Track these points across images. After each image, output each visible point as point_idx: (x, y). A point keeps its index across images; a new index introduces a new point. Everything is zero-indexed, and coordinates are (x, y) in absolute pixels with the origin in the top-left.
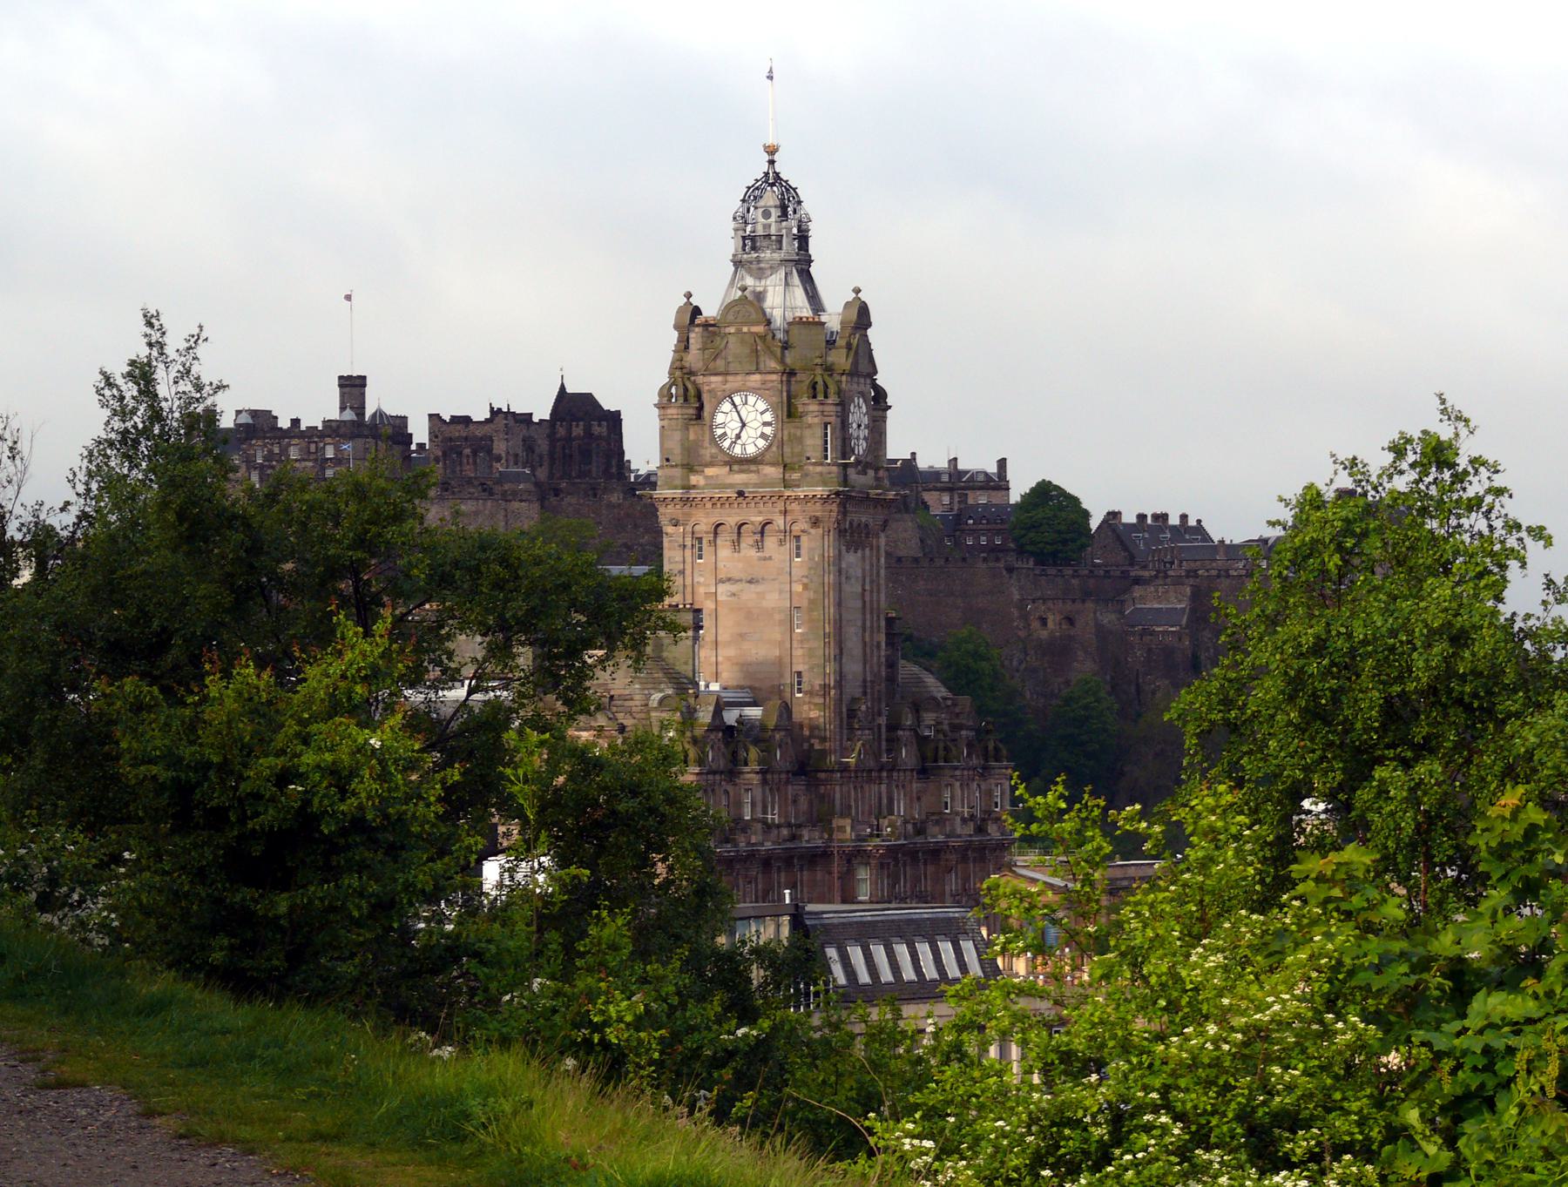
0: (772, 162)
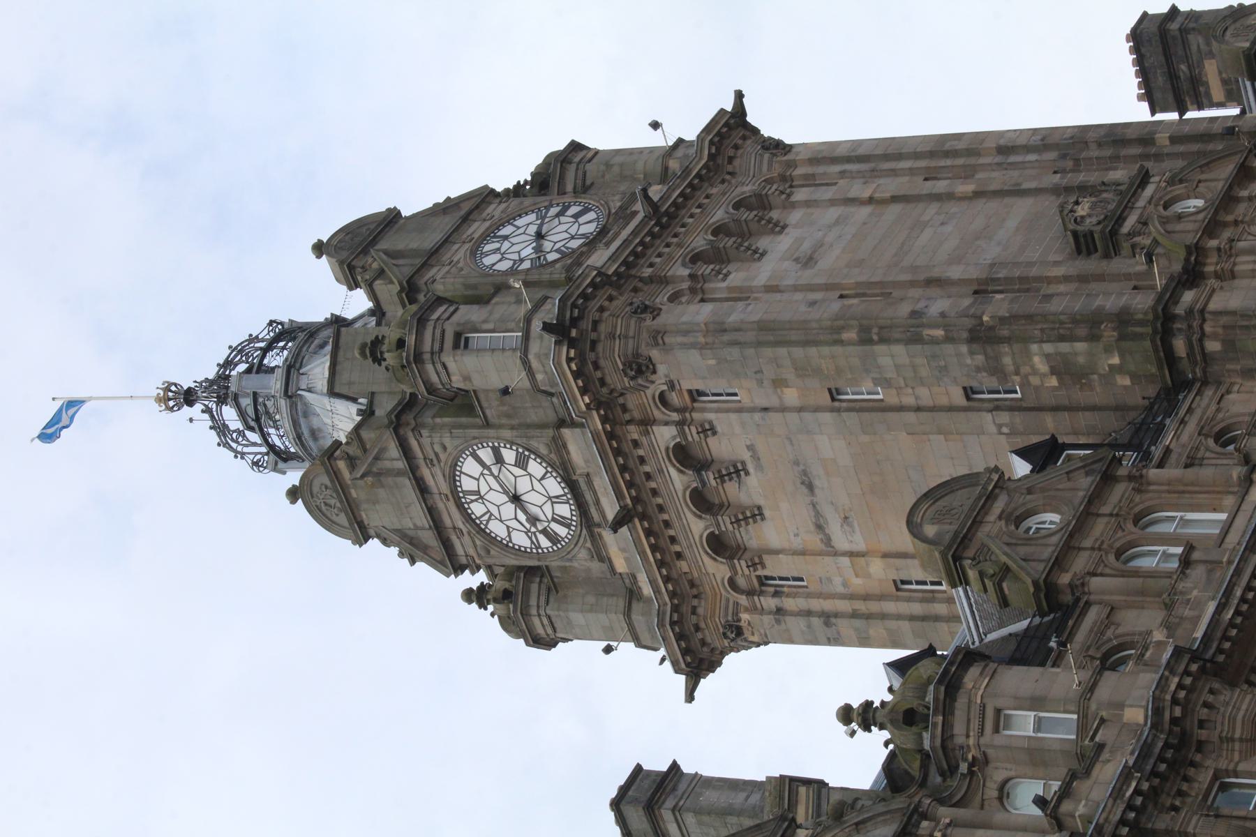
0: (189, 397)
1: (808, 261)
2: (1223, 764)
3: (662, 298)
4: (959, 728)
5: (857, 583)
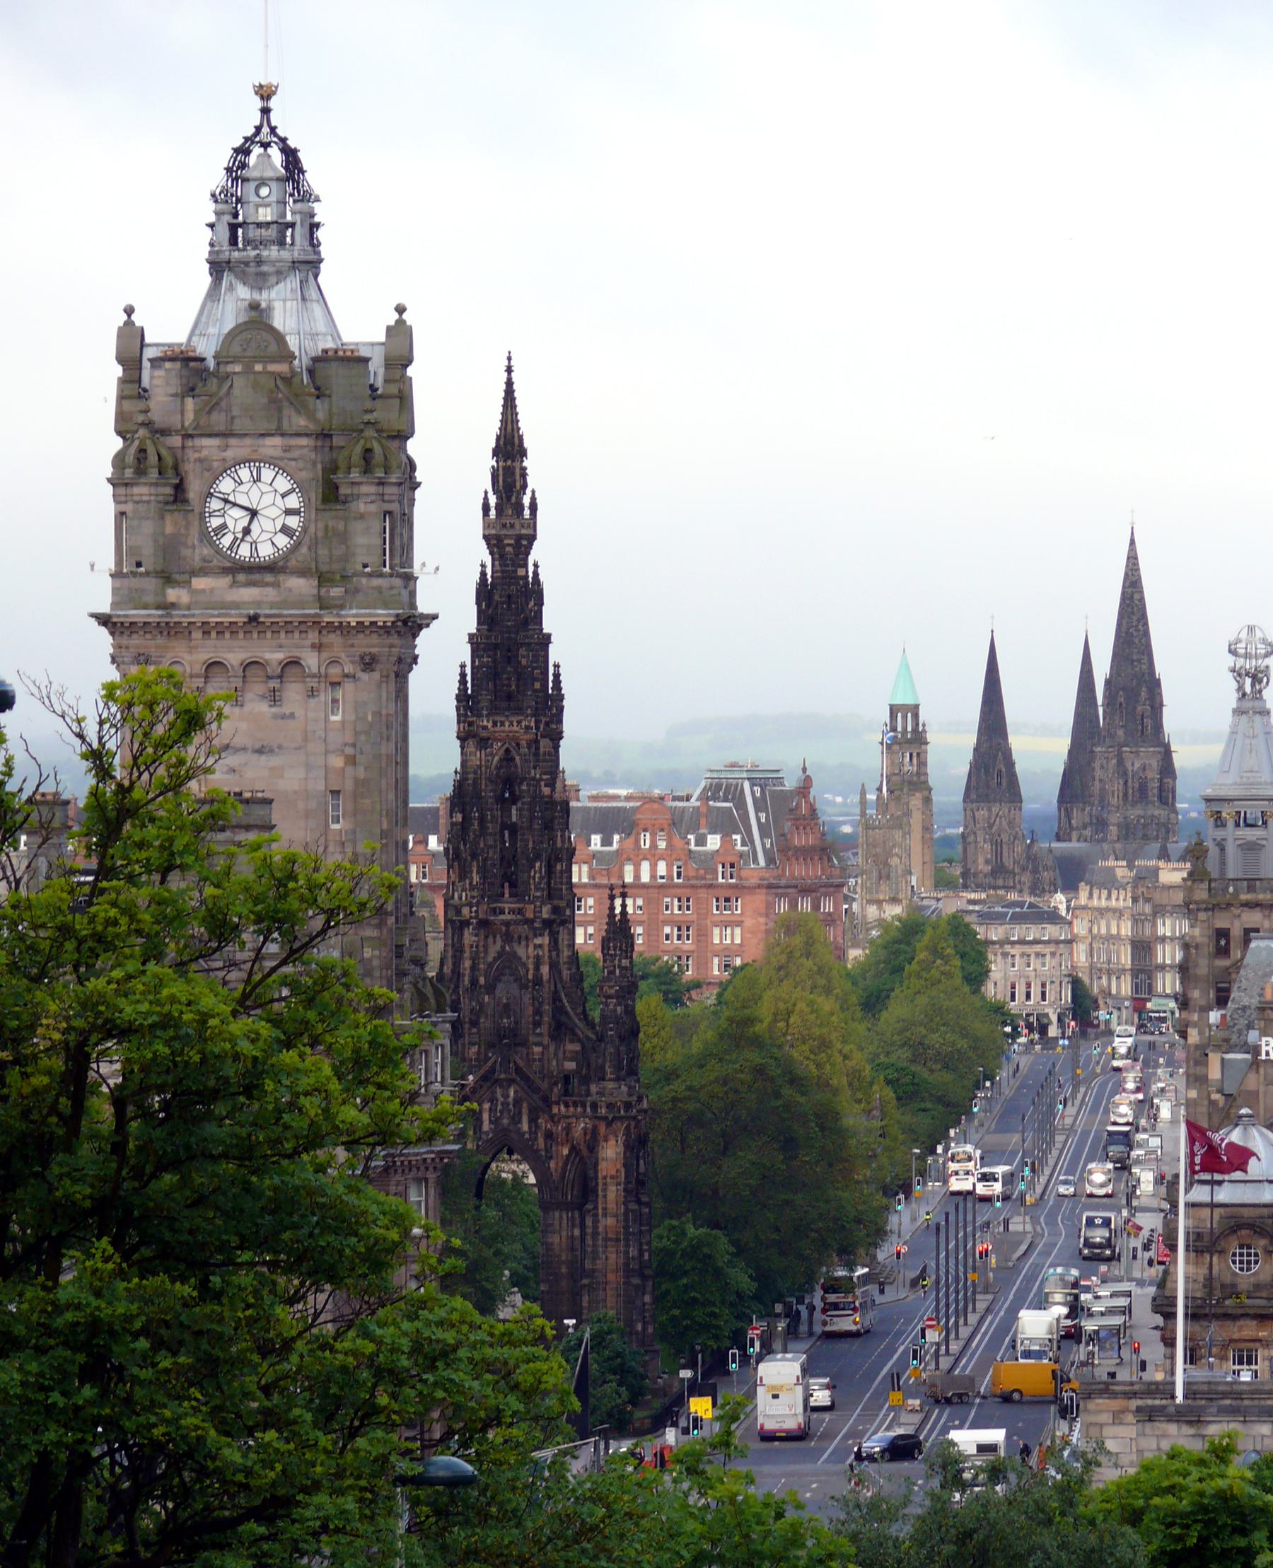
0: (266, 111)
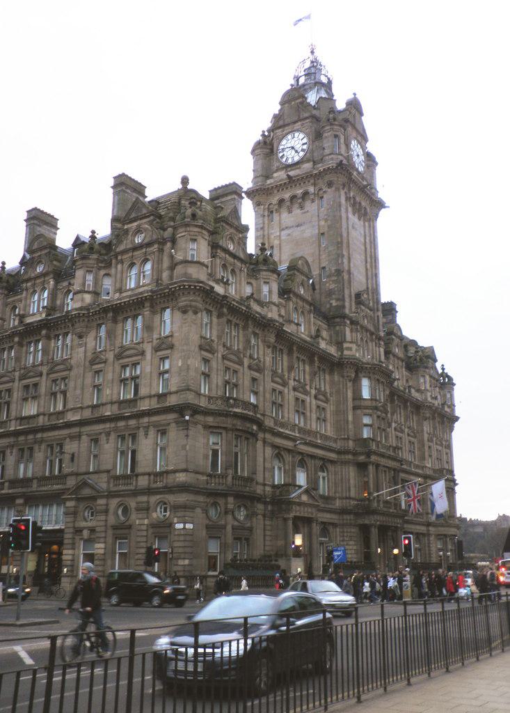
0: (312, 52)
1: (353, 227)
2: (260, 335)
3: (345, 190)
4: (264, 273)
5: (272, 237)
